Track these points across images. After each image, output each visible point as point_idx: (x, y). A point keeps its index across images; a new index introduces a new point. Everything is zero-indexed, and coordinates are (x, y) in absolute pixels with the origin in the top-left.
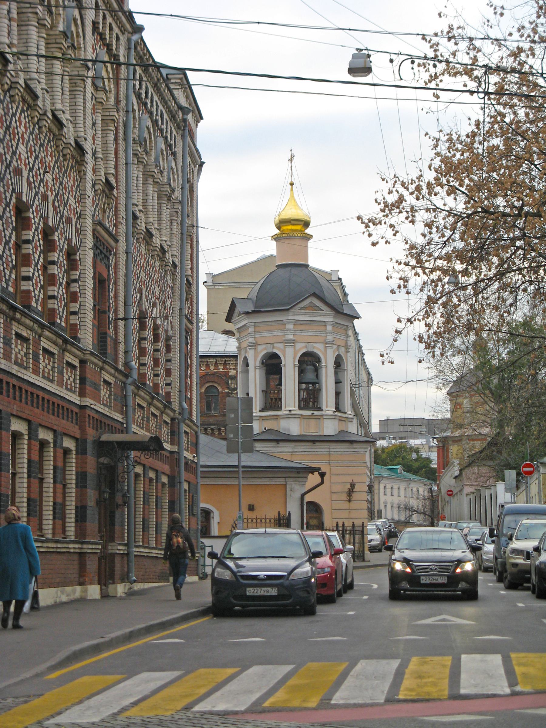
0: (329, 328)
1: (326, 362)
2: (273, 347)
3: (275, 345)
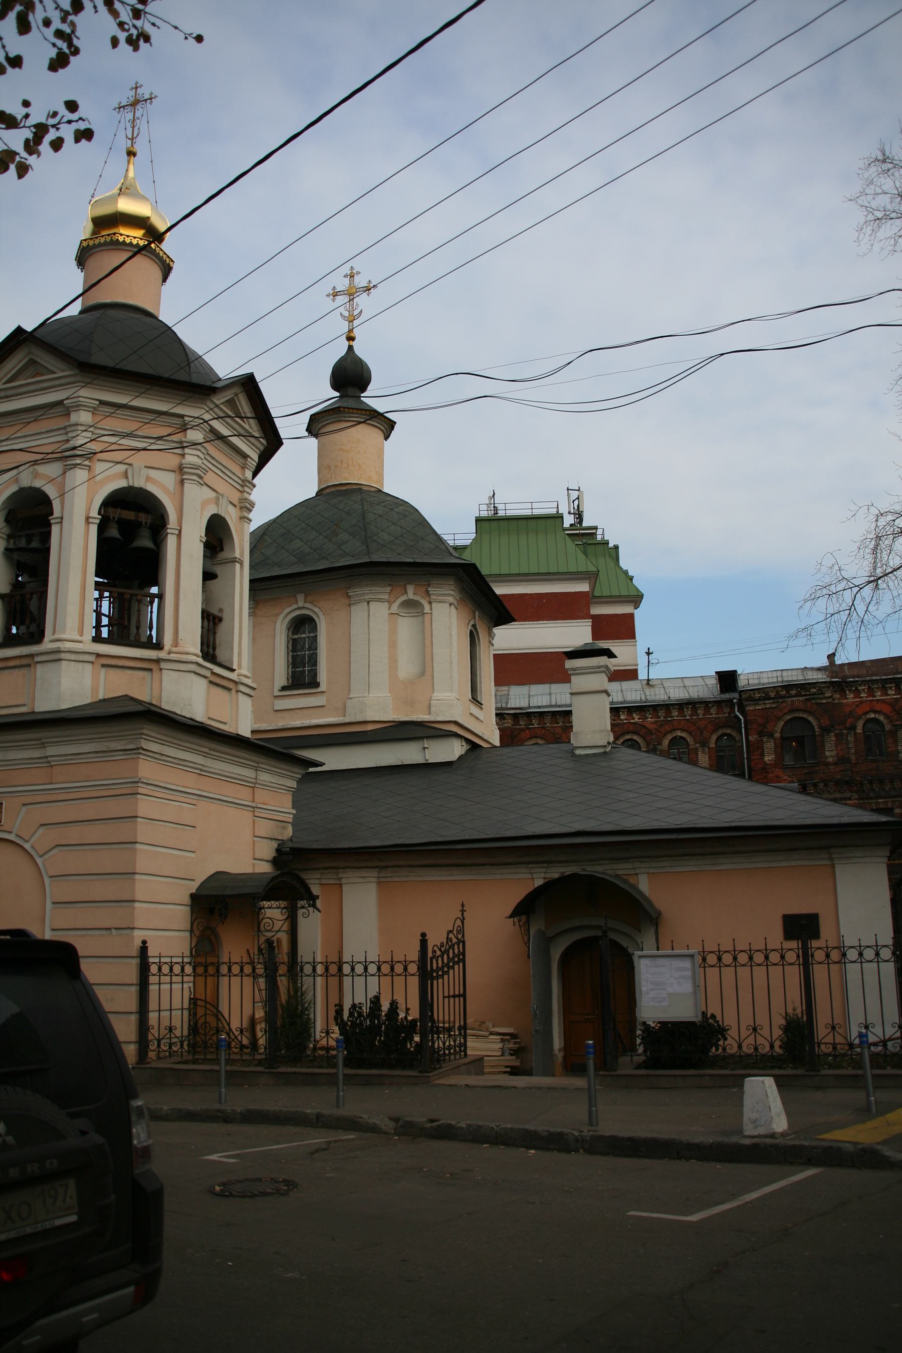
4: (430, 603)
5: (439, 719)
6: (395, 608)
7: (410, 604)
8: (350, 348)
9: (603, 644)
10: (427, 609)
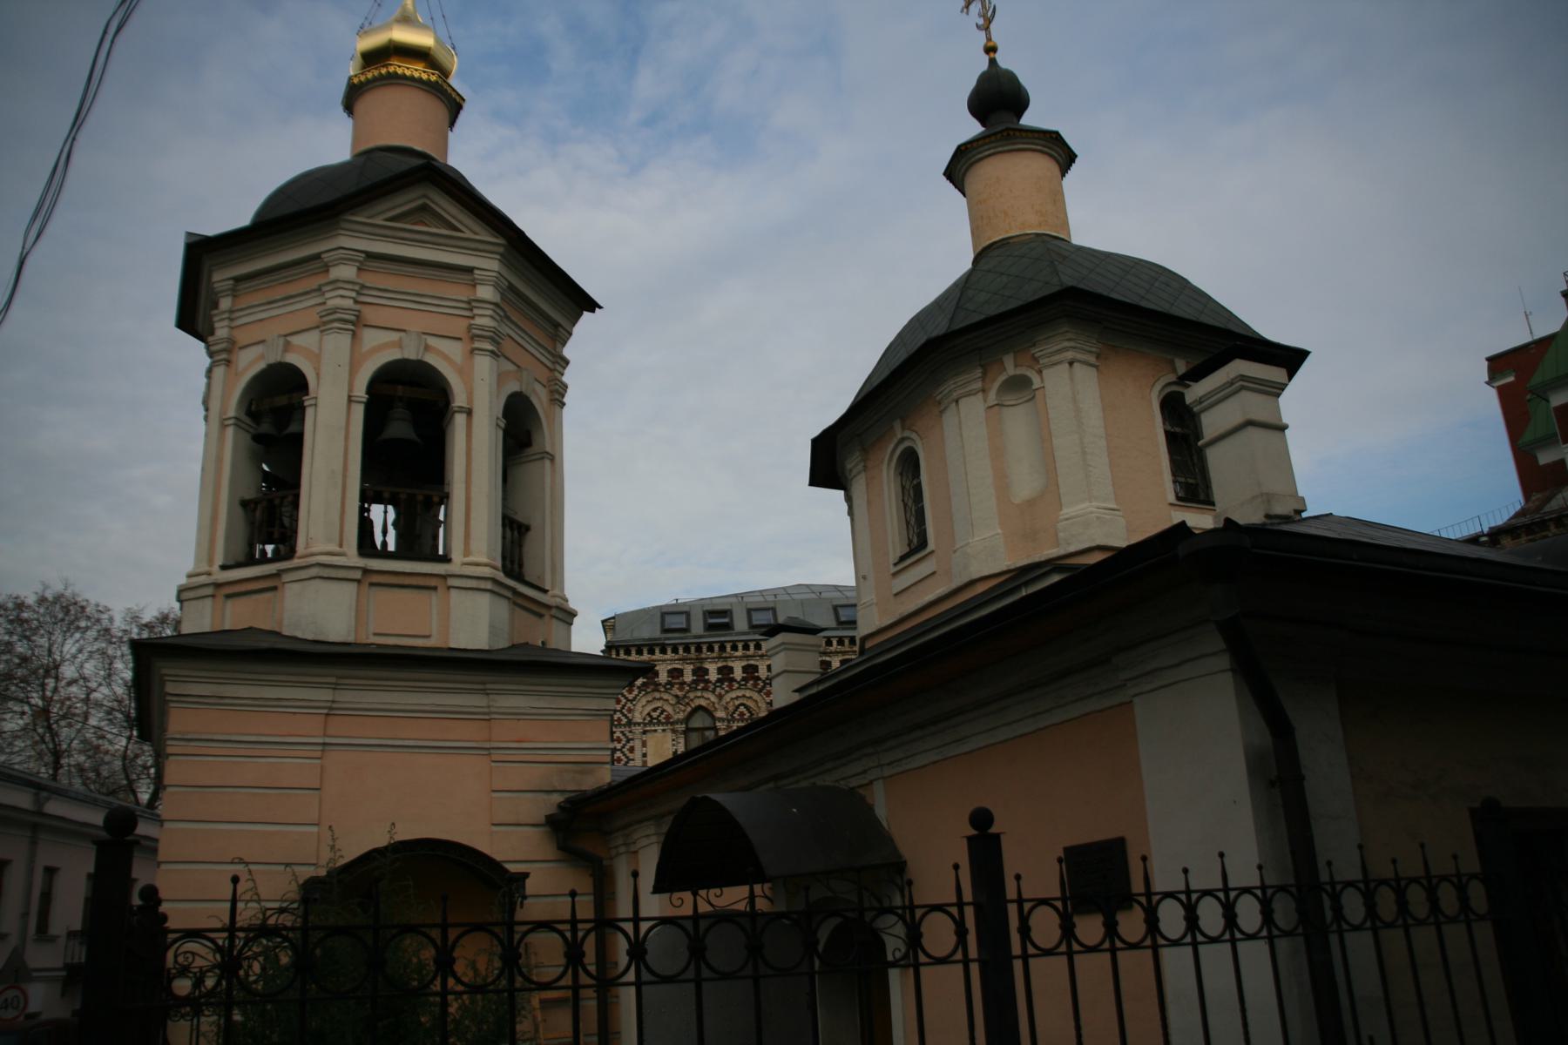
0: (486, 292)
1: (470, 398)
2: (287, 347)
3: (295, 340)
4: (1040, 372)
5: (1072, 549)
6: (992, 397)
7: (1019, 384)
8: (993, 62)
9: (358, 307)
10: (1037, 382)
